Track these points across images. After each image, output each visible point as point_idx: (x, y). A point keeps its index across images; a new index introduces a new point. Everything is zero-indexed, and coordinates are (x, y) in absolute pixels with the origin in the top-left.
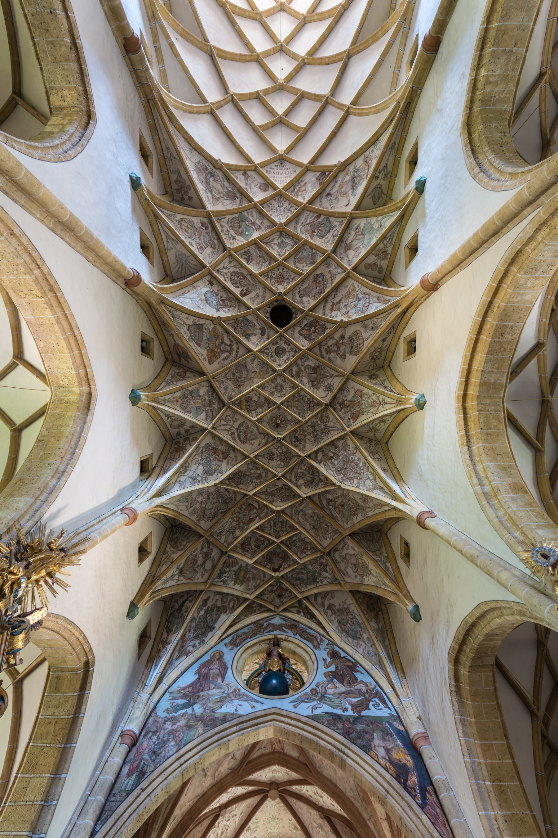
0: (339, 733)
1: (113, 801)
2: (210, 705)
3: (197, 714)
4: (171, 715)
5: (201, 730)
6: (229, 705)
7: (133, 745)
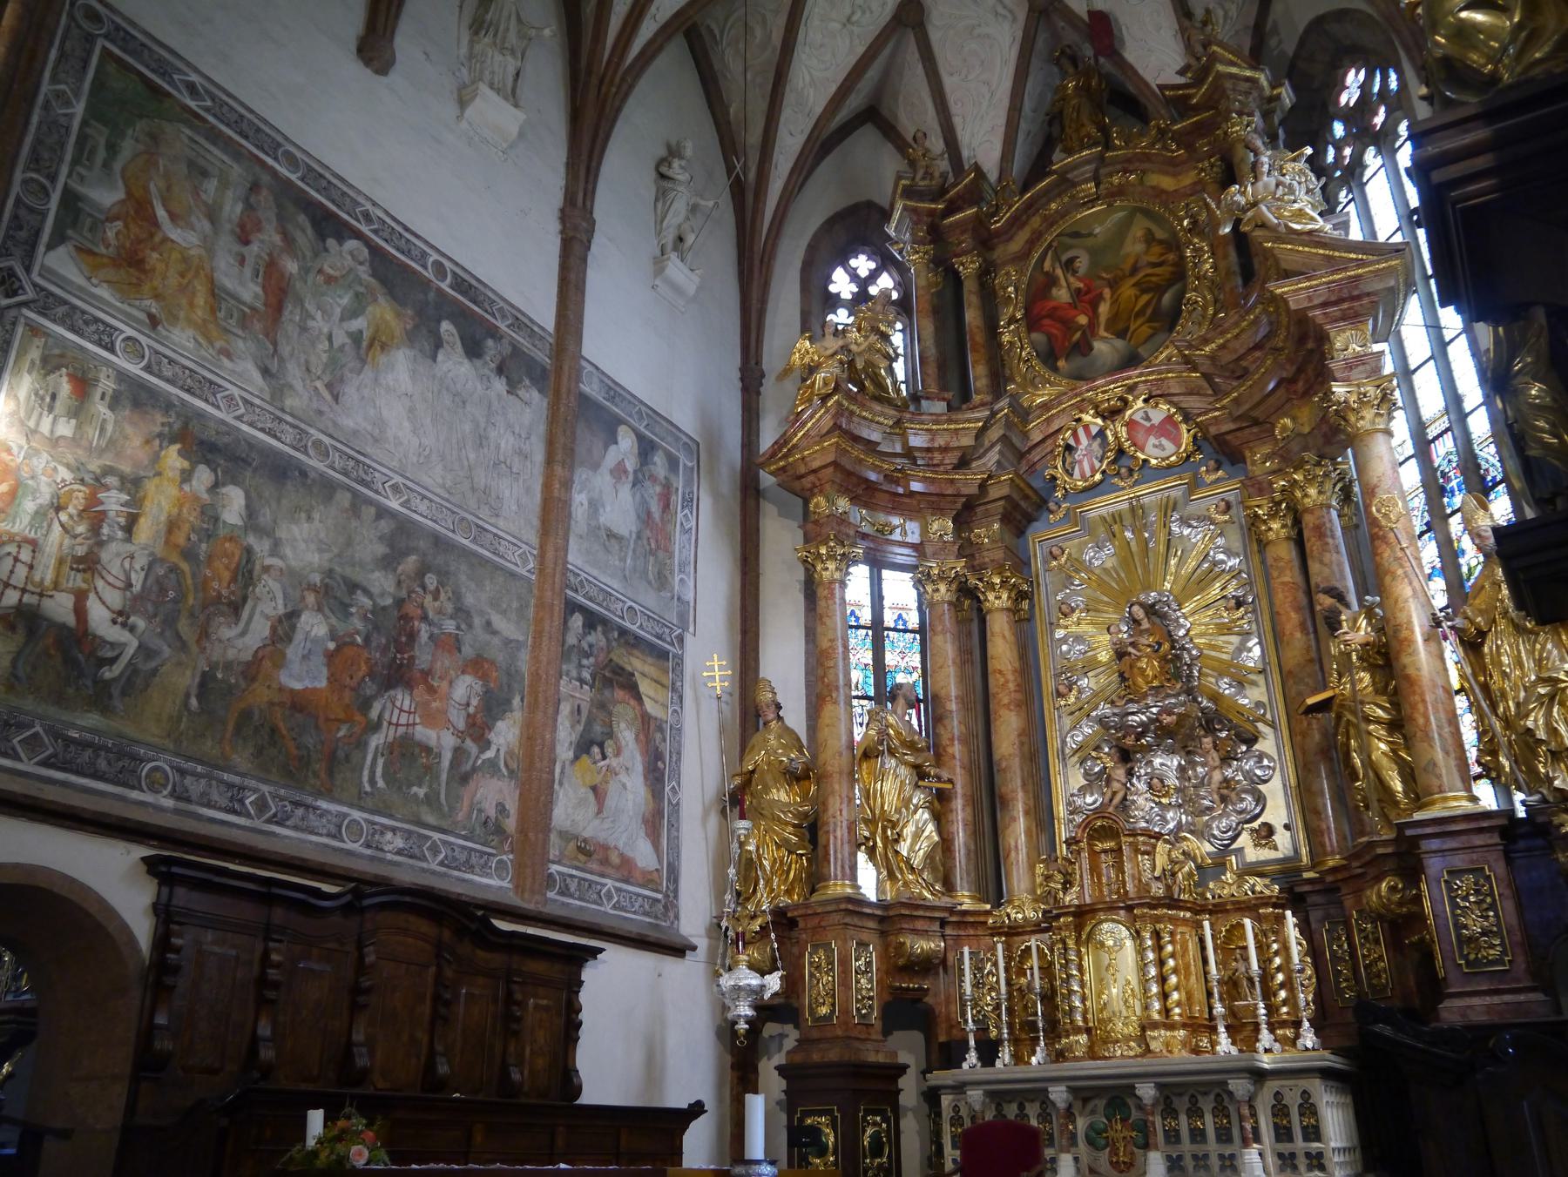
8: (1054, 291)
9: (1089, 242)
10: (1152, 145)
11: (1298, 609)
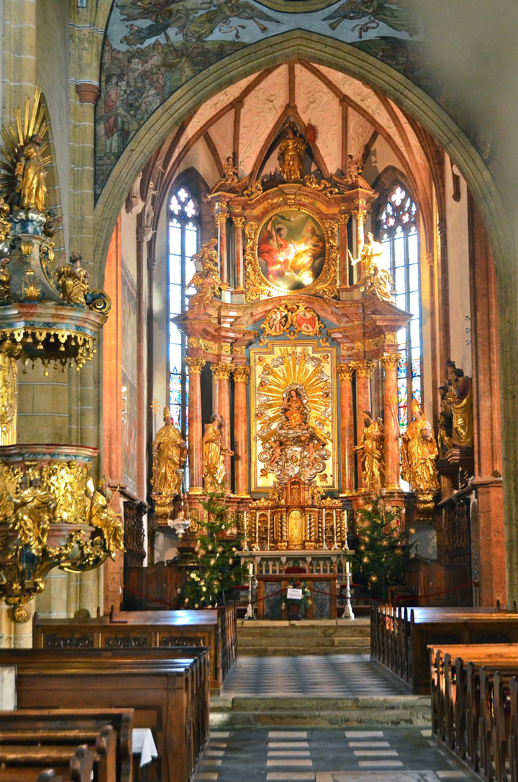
0: (398, 71)
1: (103, 165)
2: (192, 28)
3: (176, 45)
4: (135, 48)
5: (188, 71)
6: (225, 28)
7: (98, 97)
8: (271, 241)
9: (288, 223)
10: (320, 191)
11: (350, 407)
